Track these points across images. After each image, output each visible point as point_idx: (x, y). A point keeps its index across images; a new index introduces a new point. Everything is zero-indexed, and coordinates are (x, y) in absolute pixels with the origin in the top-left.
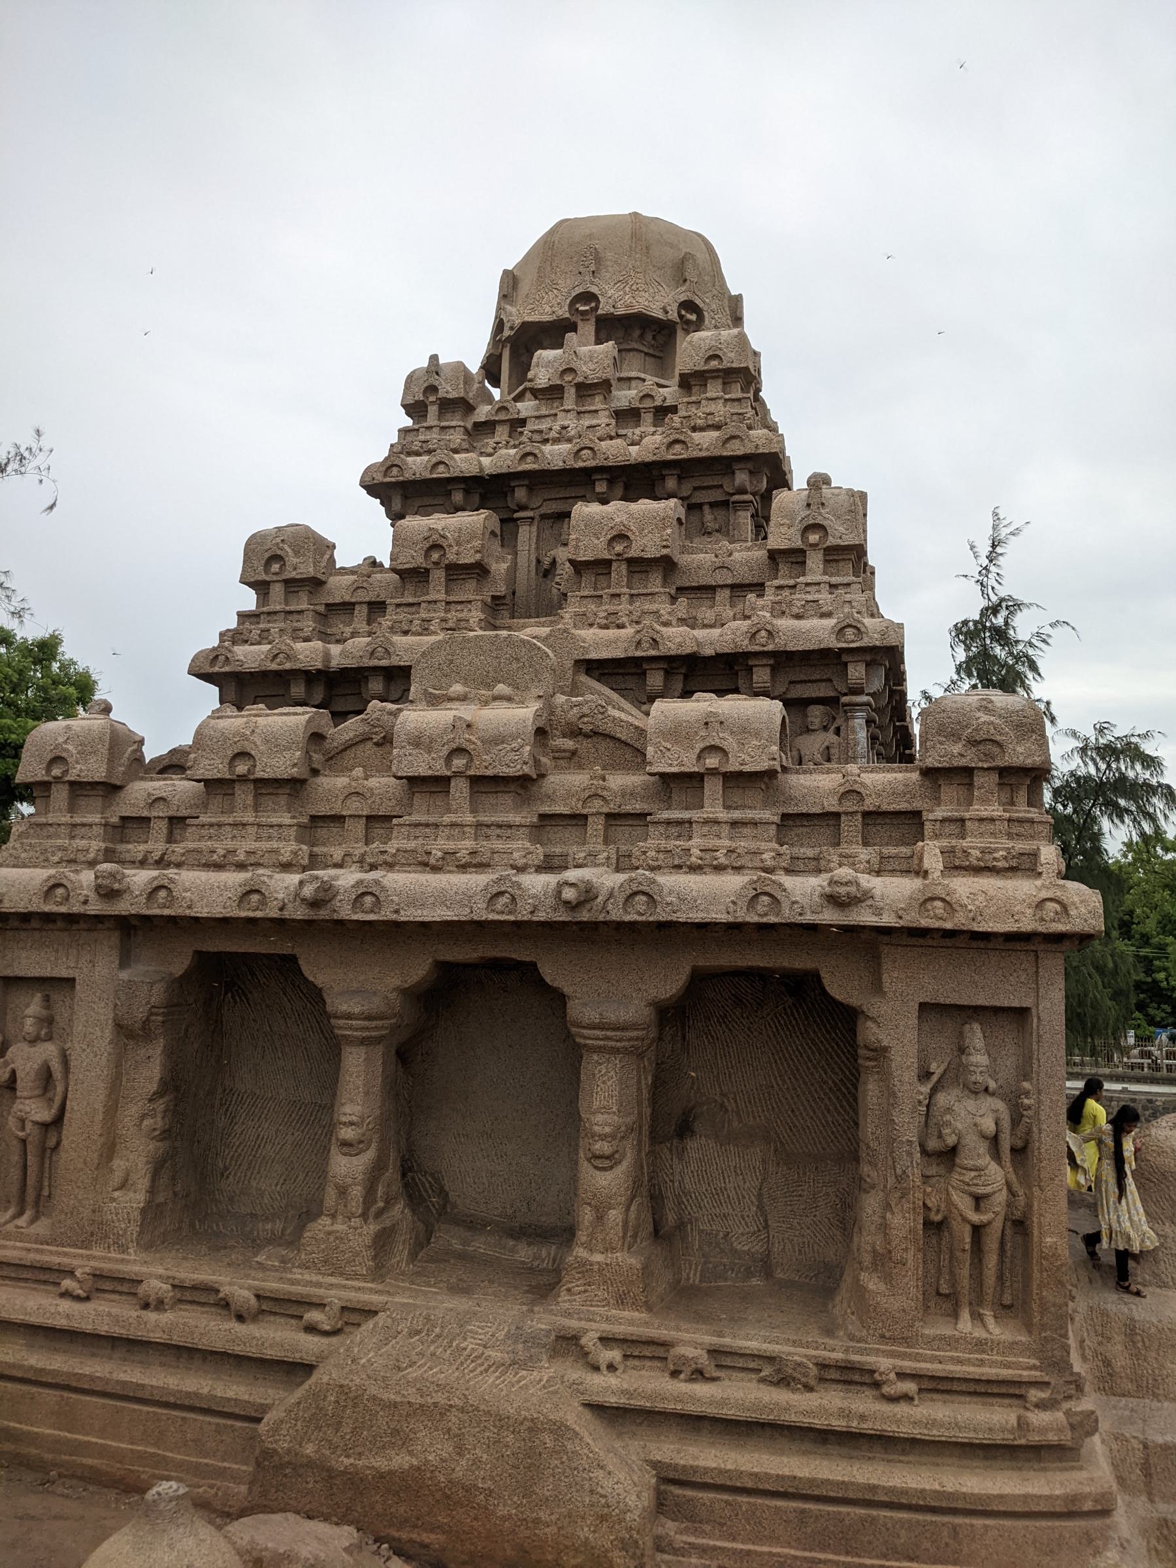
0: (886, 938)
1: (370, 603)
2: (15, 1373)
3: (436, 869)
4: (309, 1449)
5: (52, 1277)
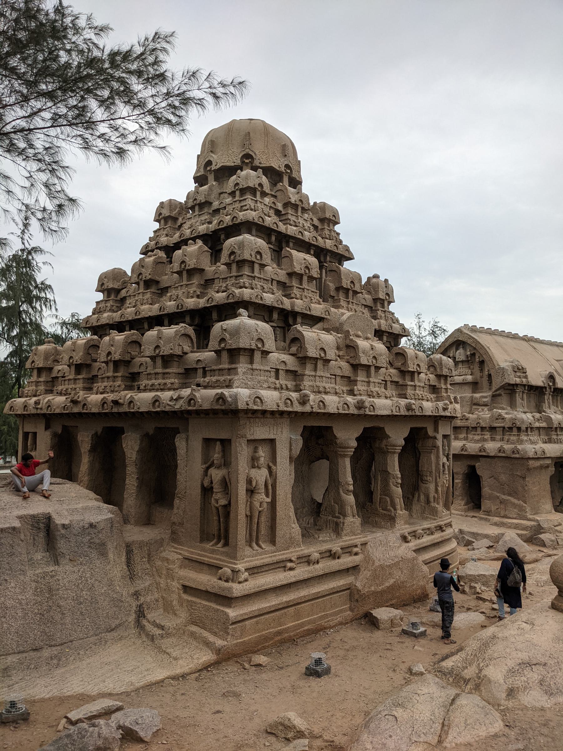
0: (442, 419)
1: (277, 281)
2: (280, 607)
3: (373, 397)
4: (373, 588)
5: (282, 565)
